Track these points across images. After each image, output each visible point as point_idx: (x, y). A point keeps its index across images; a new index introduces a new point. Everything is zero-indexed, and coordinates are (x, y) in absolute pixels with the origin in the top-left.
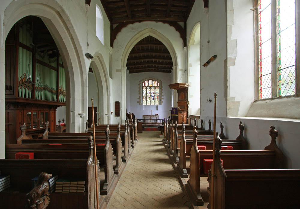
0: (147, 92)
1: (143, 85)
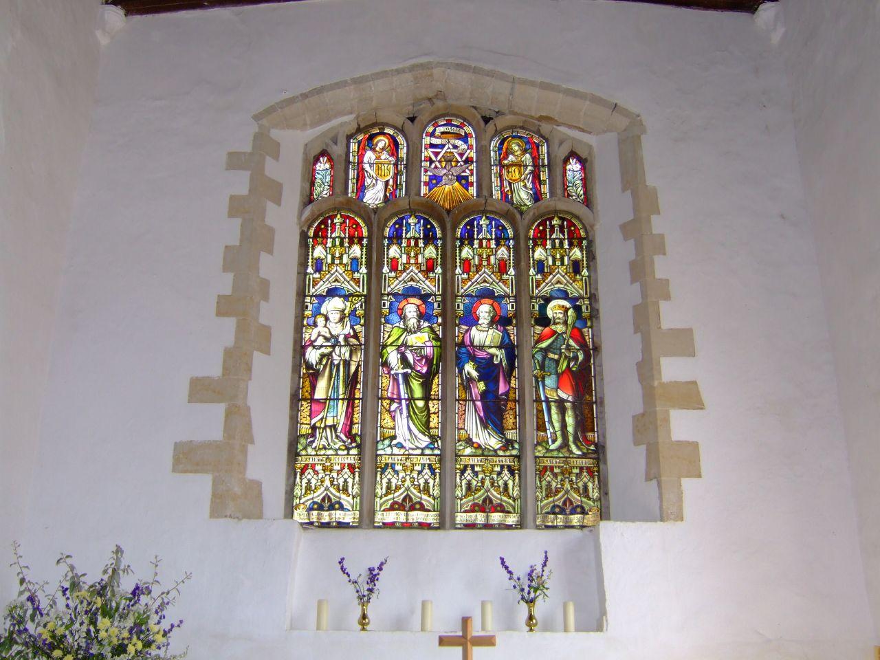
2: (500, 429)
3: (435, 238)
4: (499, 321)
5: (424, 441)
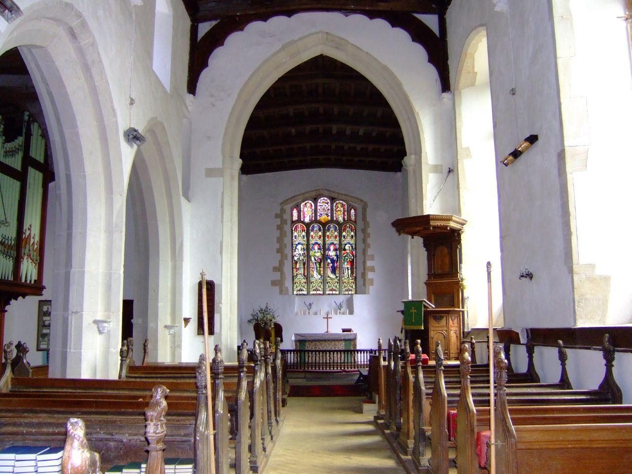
0: (308, 245)
1: (295, 218)
2: (335, 274)
3: (321, 230)
4: (335, 250)
5: (320, 277)
